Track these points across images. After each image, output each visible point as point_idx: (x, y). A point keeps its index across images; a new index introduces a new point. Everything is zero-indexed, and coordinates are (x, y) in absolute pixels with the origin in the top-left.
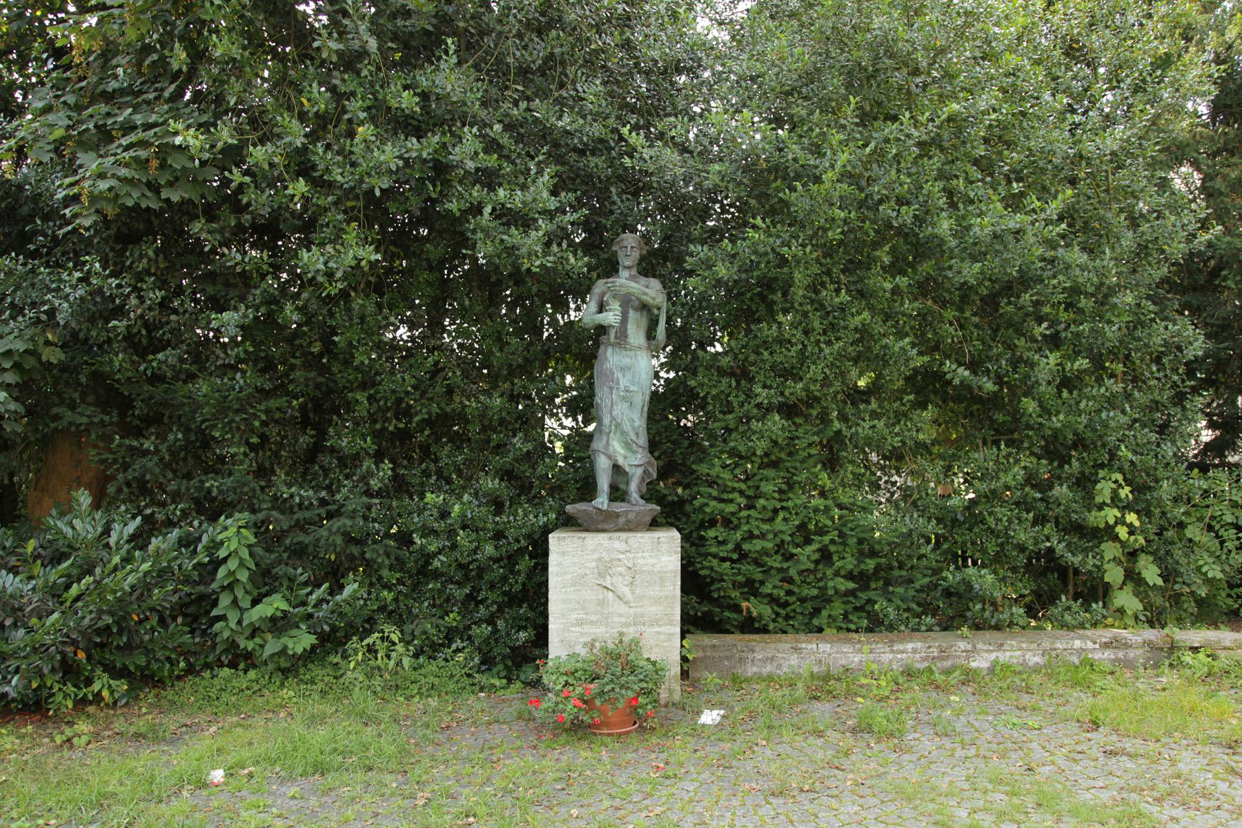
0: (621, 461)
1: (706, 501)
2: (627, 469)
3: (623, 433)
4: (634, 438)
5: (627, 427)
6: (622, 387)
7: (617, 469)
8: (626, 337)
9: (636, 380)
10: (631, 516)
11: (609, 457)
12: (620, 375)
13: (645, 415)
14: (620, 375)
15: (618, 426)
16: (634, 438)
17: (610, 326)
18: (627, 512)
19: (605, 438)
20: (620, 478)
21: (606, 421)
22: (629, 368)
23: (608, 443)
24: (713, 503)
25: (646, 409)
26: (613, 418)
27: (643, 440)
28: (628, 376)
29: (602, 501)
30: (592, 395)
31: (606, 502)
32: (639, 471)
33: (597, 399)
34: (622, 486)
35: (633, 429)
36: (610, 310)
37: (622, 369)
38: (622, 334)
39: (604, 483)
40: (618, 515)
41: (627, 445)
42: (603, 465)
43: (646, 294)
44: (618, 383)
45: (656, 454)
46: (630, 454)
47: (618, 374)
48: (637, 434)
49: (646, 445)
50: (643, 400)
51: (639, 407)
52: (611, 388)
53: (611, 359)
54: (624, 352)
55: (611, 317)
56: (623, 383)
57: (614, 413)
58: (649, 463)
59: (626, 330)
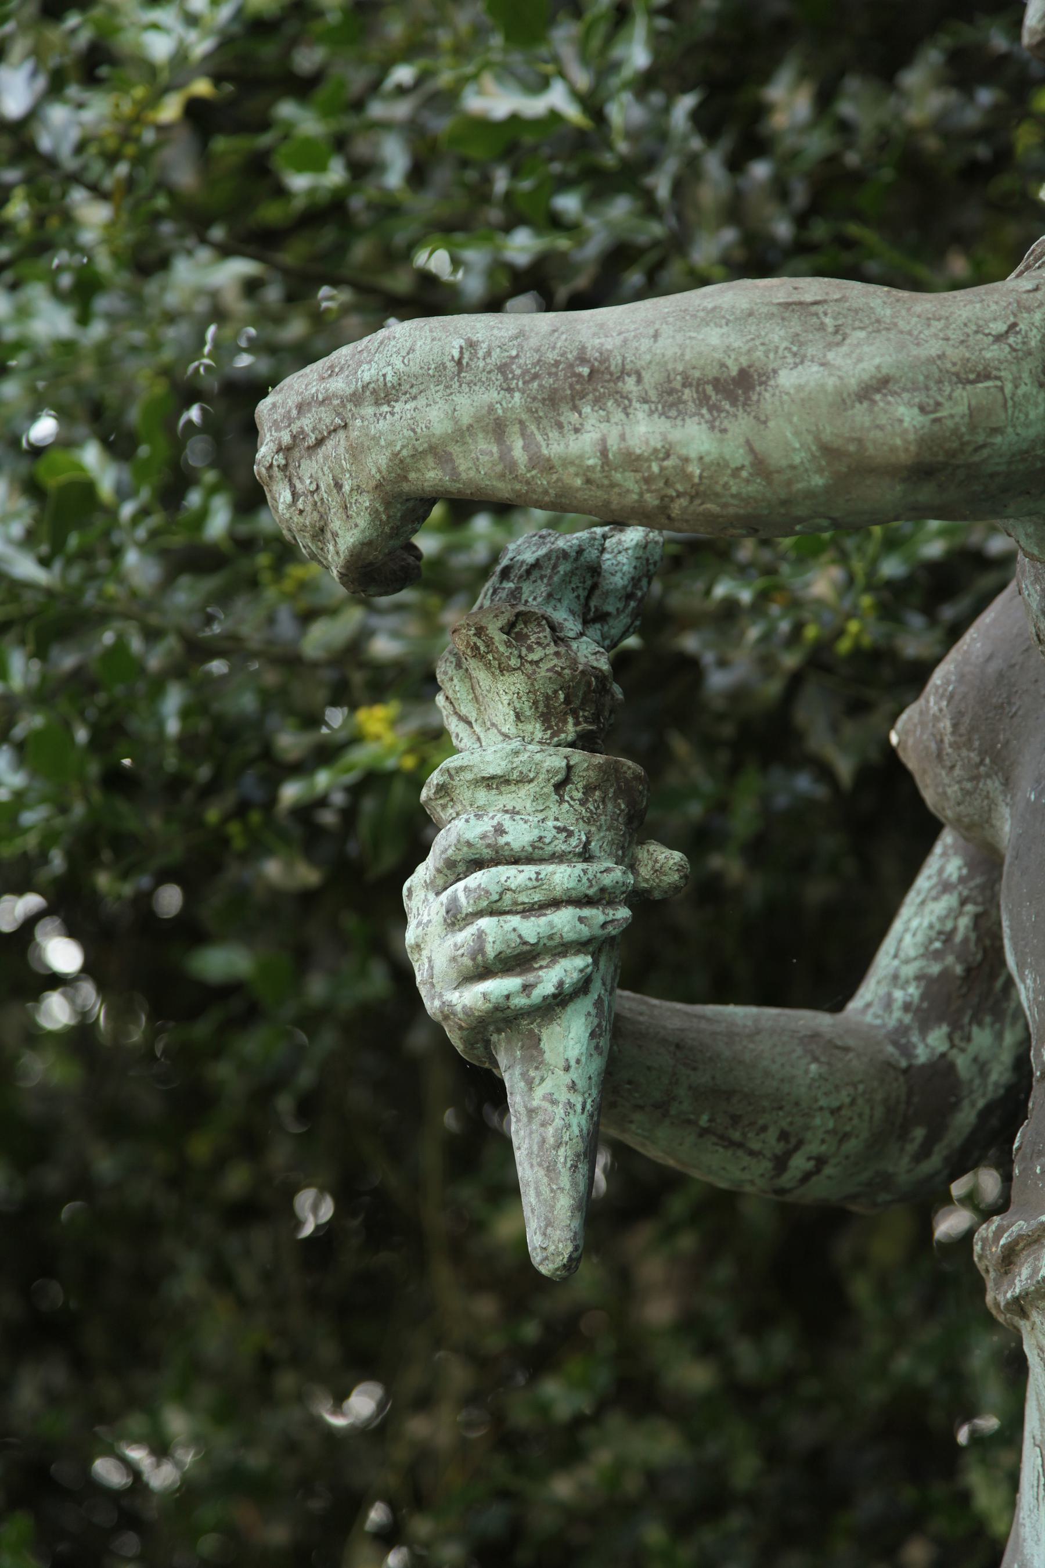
43: (593, 381)
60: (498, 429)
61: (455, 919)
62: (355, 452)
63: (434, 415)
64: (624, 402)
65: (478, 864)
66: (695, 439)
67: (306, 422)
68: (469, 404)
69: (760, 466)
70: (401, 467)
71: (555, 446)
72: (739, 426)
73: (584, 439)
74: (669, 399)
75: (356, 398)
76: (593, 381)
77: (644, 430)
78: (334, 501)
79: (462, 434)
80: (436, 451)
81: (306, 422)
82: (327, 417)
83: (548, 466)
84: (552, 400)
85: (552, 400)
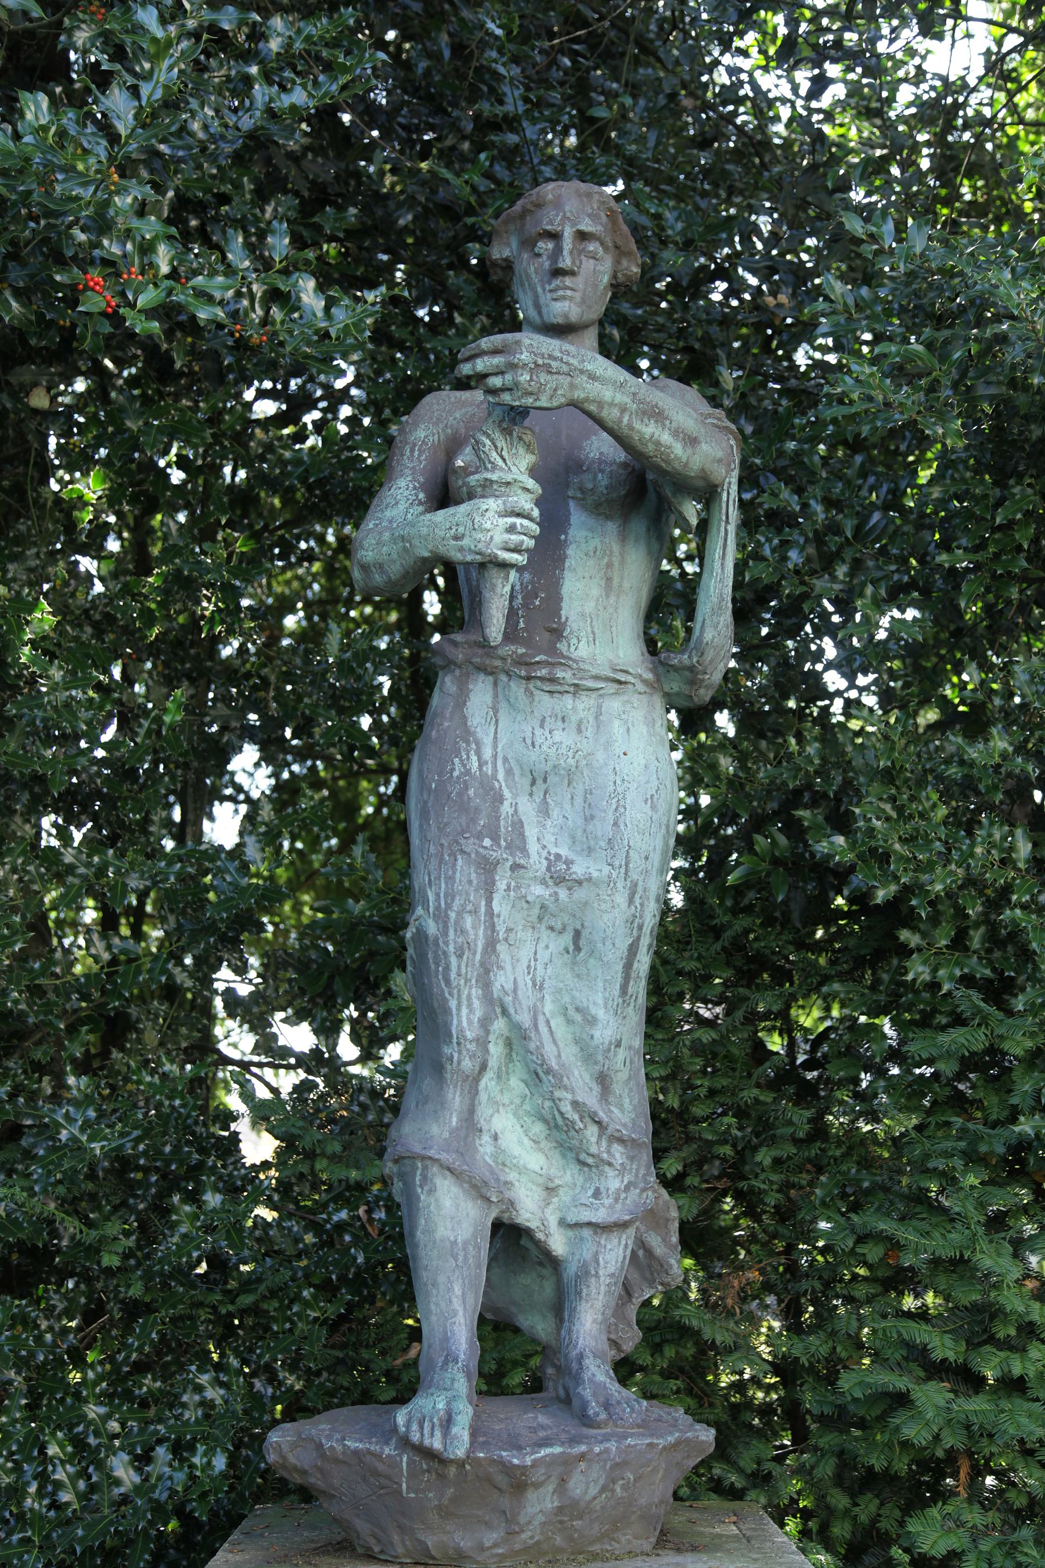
0: (530, 1209)
1: (900, 1382)
2: (558, 1244)
3: (539, 1075)
4: (591, 1099)
5: (558, 1045)
6: (536, 861)
7: (510, 1240)
8: (557, 633)
9: (603, 828)
10: (584, 1485)
11: (478, 1189)
12: (527, 809)
13: (639, 988)
14: (527, 809)
15: (518, 1040)
16: (591, 1099)
17: (489, 564)
18: (567, 1463)
19: (455, 1098)
20: (532, 1285)
21: (465, 1015)
22: (570, 776)
23: (471, 1124)
24: (933, 1396)
25: (643, 962)
26: (497, 1006)
27: (629, 1109)
28: (565, 809)
29: (447, 1411)
30: (398, 902)
31: (464, 1415)
32: (613, 1255)
33: (423, 920)
34: (538, 1324)
35: (588, 1054)
36: (487, 488)
37: (537, 779)
38: (540, 620)
39: (451, 1307)
40: (519, 1483)
41: (561, 1132)
42: (449, 1224)
43: (657, 415)
44: (518, 843)
45: (672, 1166)
46: (568, 1176)
47: (519, 804)
48: (603, 1080)
49: (643, 1130)
50: (634, 922)
51: (615, 954)
52: (488, 868)
53: (489, 730)
54: (545, 703)
55: (496, 523)
56: (544, 839)
57: (501, 981)
58: (652, 1217)
59: (555, 600)
60: (623, 410)
61: (511, 529)
62: (572, 386)
63: (608, 394)
64: (664, 426)
65: (518, 515)
66: (678, 449)
67: (554, 364)
68: (619, 398)
69: (686, 465)
70: (587, 400)
71: (637, 425)
72: (689, 451)
73: (648, 430)
74: (676, 433)
75: (582, 372)
76: (657, 415)
77: (666, 438)
78: (549, 392)
79: (612, 404)
80: (600, 404)
81: (554, 364)
82: (565, 368)
83: (630, 427)
84: (644, 413)
85: (644, 413)
